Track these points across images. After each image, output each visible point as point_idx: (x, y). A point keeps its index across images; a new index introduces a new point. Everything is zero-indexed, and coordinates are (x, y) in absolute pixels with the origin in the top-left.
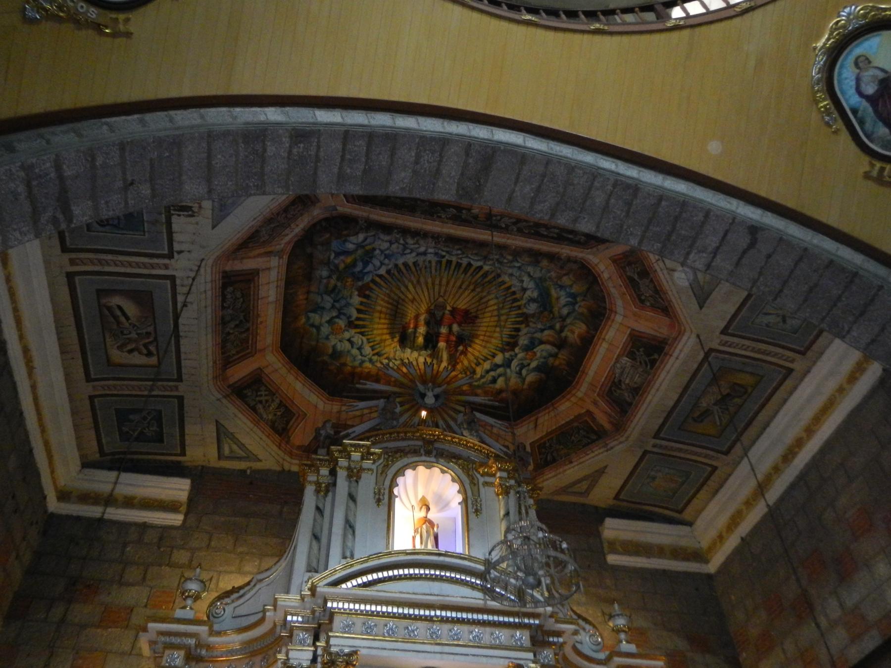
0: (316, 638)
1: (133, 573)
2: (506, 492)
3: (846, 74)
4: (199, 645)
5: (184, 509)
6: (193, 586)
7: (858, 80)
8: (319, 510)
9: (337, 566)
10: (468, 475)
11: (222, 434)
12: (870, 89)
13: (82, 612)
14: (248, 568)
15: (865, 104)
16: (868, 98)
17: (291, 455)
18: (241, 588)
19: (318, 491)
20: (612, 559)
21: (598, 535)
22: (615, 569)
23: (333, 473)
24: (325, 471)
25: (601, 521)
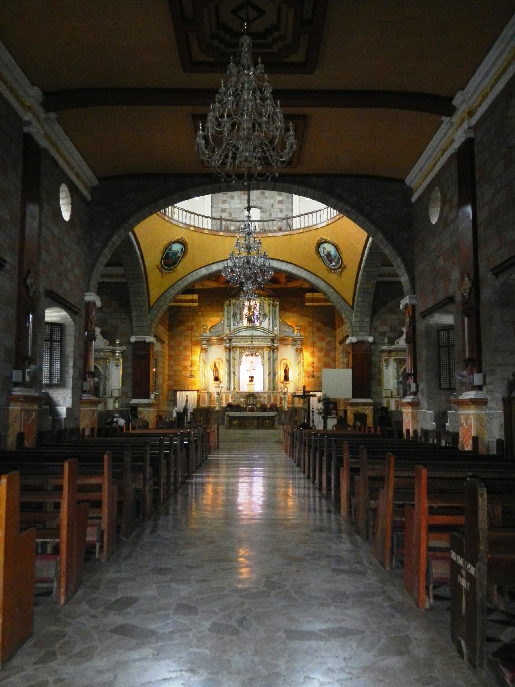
0: (230, 342)
1: (190, 318)
2: (269, 305)
3: (321, 250)
4: (209, 339)
5: (198, 301)
6: (205, 327)
7: (324, 252)
8: (228, 312)
9: (232, 328)
10: (261, 301)
11: (202, 285)
12: (326, 254)
13: (182, 328)
14: (215, 315)
15: (325, 257)
16: (325, 255)
17: (220, 284)
18: (214, 326)
19: (227, 306)
20: (307, 304)
21: (304, 297)
22: (308, 306)
23: (230, 302)
24: (228, 302)
25: (305, 293)
